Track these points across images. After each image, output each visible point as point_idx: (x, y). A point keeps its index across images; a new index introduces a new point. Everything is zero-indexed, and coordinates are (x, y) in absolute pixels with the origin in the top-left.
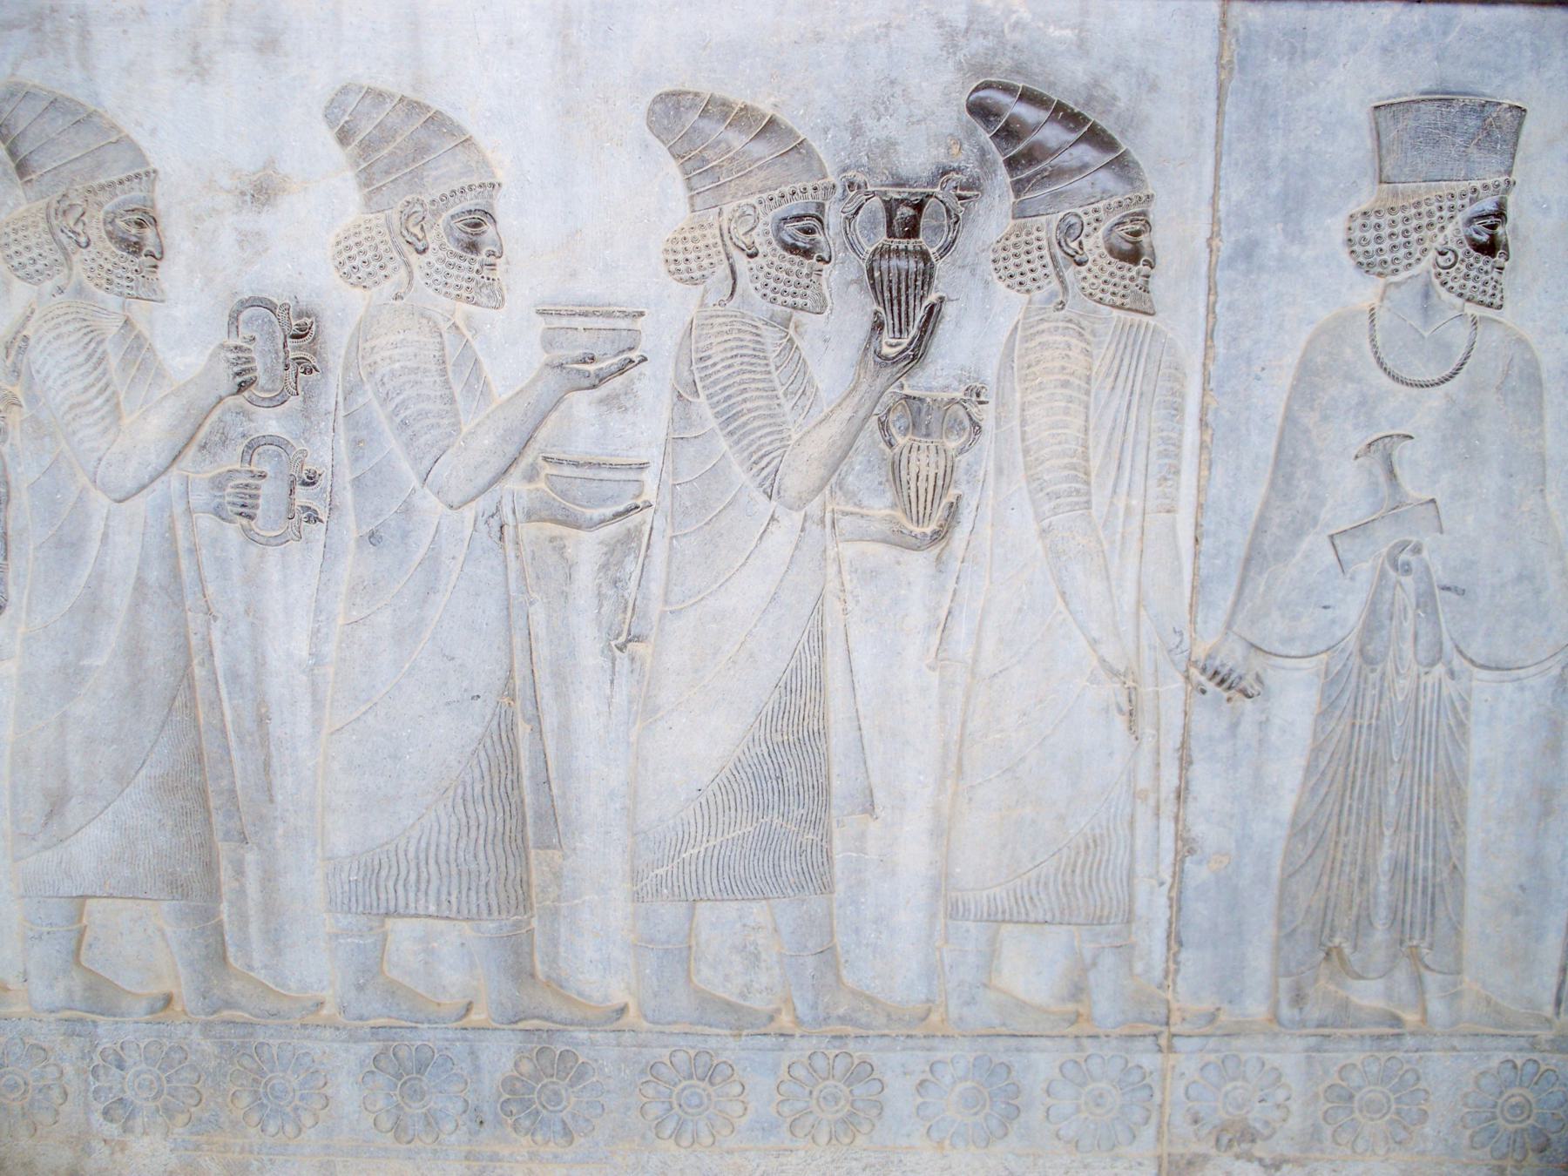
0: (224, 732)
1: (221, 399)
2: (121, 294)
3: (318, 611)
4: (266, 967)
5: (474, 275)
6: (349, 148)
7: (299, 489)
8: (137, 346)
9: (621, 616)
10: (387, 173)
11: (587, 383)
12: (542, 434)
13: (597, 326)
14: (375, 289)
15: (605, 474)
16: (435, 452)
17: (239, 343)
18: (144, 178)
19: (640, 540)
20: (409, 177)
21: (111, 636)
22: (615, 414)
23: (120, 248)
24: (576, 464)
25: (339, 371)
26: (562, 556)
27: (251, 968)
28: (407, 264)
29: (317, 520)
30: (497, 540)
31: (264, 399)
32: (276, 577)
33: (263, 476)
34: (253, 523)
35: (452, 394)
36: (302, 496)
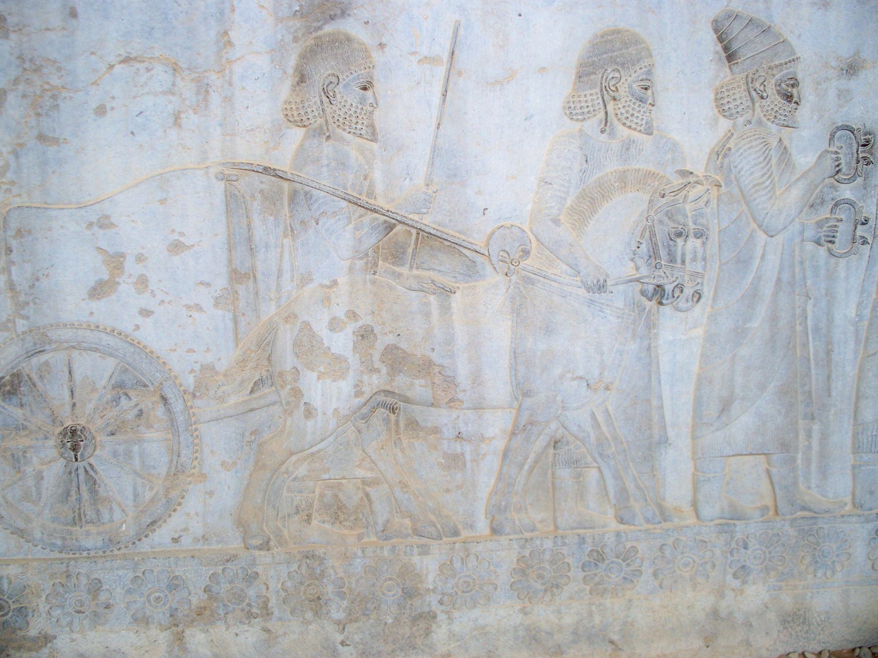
0: (809, 360)
4: (818, 486)
21: (762, 310)
23: (783, 99)
27: (809, 488)
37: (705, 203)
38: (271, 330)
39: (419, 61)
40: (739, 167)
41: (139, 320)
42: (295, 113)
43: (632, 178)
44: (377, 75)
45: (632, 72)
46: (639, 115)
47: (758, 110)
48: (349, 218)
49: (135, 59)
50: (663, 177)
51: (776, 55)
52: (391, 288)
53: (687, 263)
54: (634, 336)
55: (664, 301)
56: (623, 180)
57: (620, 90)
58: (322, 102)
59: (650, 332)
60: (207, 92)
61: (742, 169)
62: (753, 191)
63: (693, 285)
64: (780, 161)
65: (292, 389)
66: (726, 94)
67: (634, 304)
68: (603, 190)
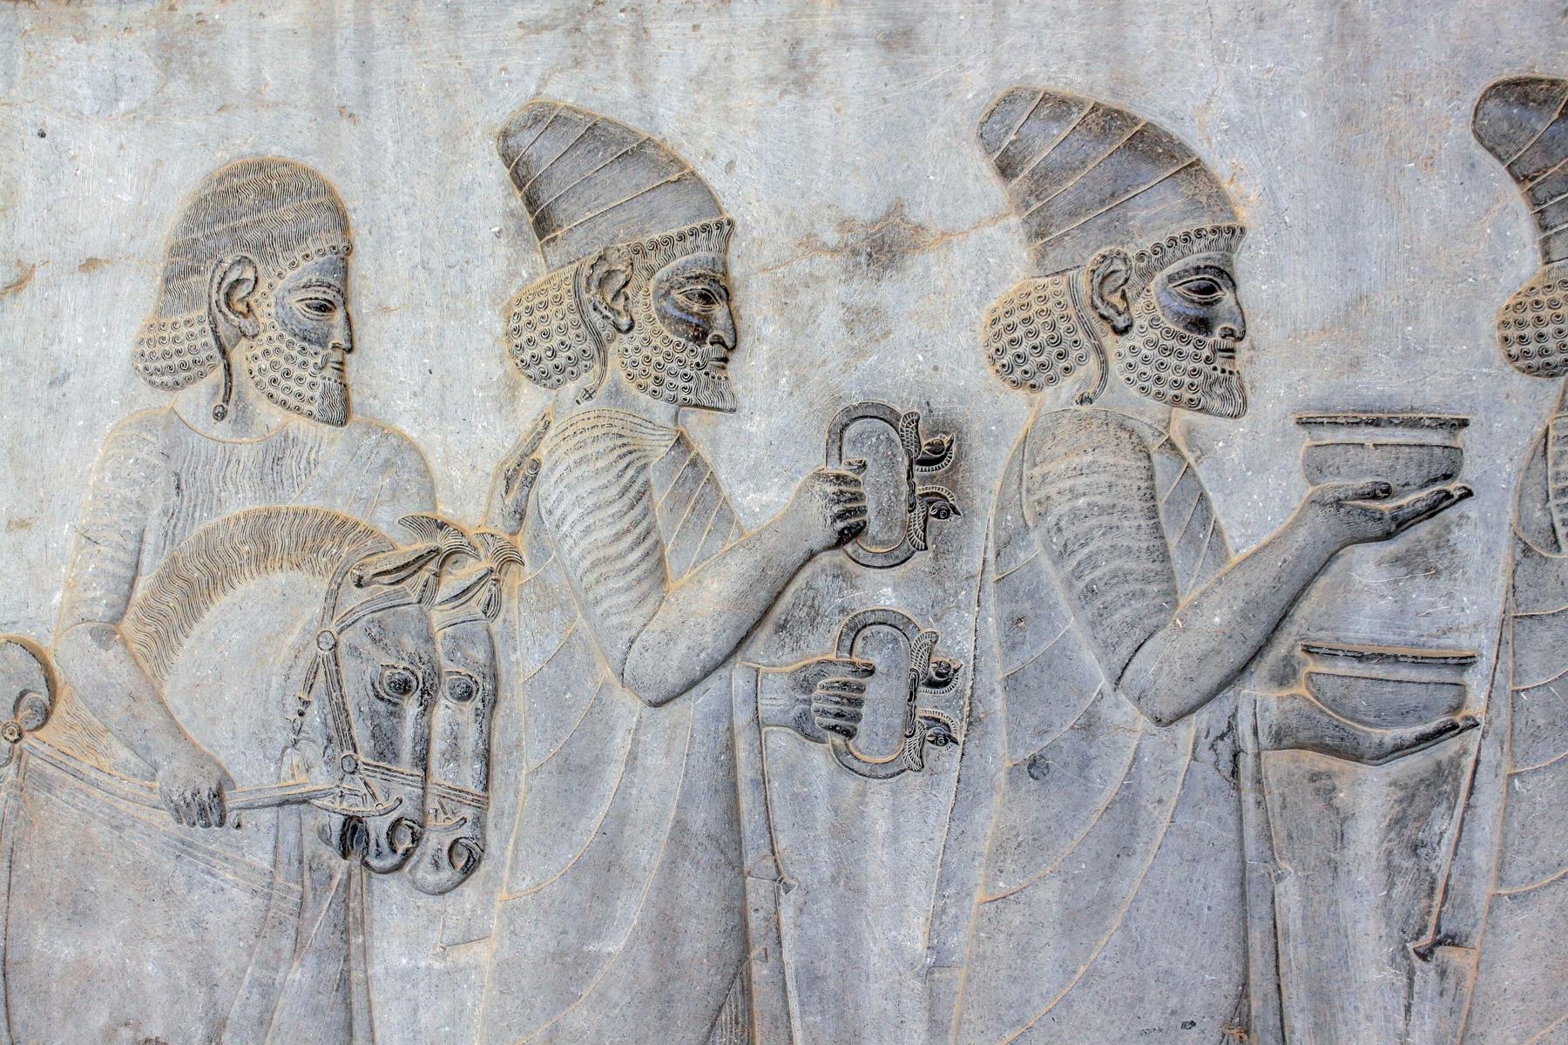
1: (812, 555)
2: (674, 400)
3: (944, 881)
5: (1200, 365)
6: (1015, 181)
9: (1425, 902)
10: (1073, 215)
11: (1377, 529)
12: (1304, 609)
13: (1393, 440)
14: (1049, 390)
15: (1405, 673)
16: (1138, 634)
17: (843, 470)
18: (715, 232)
19: (1457, 779)
20: (1104, 220)
22: (1420, 576)
23: (676, 332)
24: (1360, 657)
25: (992, 512)
26: (1329, 804)
28: (1100, 350)
29: (949, 739)
30: (1227, 774)
31: (875, 554)
32: (882, 826)
33: (870, 671)
34: (850, 743)
35: (1165, 545)
36: (928, 703)
37: (481, 607)
40: (558, 513)
43: (285, 533)
45: (284, 264)
46: (305, 374)
47: (614, 361)
51: (652, 216)
54: (297, 949)
55: (374, 863)
57: (258, 312)
59: (347, 942)
61: (563, 518)
62: (591, 577)
63: (448, 823)
66: (525, 318)
67: (301, 862)
68: (213, 561)
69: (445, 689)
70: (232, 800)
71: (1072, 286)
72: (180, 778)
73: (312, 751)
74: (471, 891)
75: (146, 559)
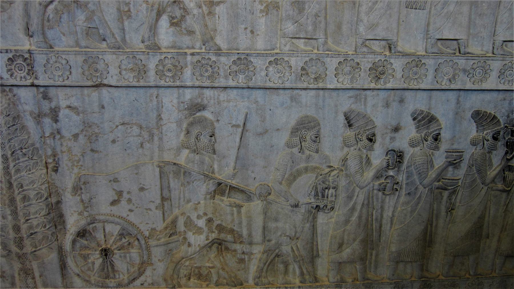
7: (395, 185)
8: (368, 160)
10: (423, 126)
15: (454, 181)
21: (356, 214)
22: (456, 170)
25: (406, 163)
28: (423, 143)
33: (388, 183)
38: (177, 218)
39: (232, 126)
41: (129, 213)
42: (186, 145)
44: (217, 131)
47: (359, 145)
48: (205, 182)
49: (126, 124)
50: (321, 168)
51: (367, 125)
52: (220, 205)
53: (329, 198)
54: (308, 221)
56: (306, 169)
58: (195, 141)
60: (153, 136)
64: (366, 162)
65: (183, 237)
69: (331, 188)
70: (299, 204)
71: (421, 136)
72: (292, 202)
73: (312, 197)
74: (332, 213)
75: (287, 172)
